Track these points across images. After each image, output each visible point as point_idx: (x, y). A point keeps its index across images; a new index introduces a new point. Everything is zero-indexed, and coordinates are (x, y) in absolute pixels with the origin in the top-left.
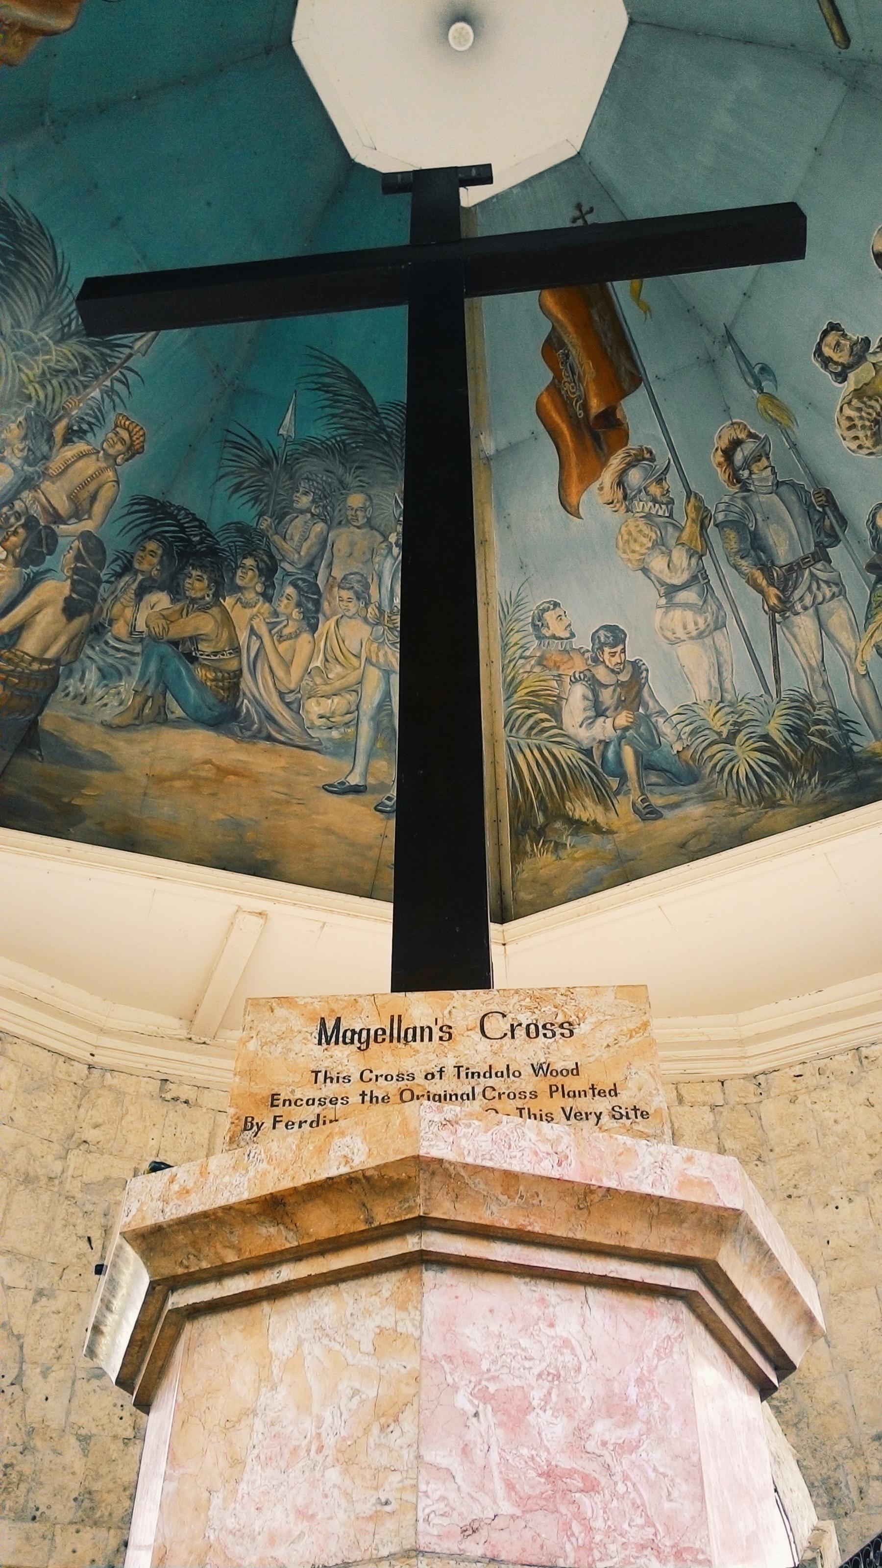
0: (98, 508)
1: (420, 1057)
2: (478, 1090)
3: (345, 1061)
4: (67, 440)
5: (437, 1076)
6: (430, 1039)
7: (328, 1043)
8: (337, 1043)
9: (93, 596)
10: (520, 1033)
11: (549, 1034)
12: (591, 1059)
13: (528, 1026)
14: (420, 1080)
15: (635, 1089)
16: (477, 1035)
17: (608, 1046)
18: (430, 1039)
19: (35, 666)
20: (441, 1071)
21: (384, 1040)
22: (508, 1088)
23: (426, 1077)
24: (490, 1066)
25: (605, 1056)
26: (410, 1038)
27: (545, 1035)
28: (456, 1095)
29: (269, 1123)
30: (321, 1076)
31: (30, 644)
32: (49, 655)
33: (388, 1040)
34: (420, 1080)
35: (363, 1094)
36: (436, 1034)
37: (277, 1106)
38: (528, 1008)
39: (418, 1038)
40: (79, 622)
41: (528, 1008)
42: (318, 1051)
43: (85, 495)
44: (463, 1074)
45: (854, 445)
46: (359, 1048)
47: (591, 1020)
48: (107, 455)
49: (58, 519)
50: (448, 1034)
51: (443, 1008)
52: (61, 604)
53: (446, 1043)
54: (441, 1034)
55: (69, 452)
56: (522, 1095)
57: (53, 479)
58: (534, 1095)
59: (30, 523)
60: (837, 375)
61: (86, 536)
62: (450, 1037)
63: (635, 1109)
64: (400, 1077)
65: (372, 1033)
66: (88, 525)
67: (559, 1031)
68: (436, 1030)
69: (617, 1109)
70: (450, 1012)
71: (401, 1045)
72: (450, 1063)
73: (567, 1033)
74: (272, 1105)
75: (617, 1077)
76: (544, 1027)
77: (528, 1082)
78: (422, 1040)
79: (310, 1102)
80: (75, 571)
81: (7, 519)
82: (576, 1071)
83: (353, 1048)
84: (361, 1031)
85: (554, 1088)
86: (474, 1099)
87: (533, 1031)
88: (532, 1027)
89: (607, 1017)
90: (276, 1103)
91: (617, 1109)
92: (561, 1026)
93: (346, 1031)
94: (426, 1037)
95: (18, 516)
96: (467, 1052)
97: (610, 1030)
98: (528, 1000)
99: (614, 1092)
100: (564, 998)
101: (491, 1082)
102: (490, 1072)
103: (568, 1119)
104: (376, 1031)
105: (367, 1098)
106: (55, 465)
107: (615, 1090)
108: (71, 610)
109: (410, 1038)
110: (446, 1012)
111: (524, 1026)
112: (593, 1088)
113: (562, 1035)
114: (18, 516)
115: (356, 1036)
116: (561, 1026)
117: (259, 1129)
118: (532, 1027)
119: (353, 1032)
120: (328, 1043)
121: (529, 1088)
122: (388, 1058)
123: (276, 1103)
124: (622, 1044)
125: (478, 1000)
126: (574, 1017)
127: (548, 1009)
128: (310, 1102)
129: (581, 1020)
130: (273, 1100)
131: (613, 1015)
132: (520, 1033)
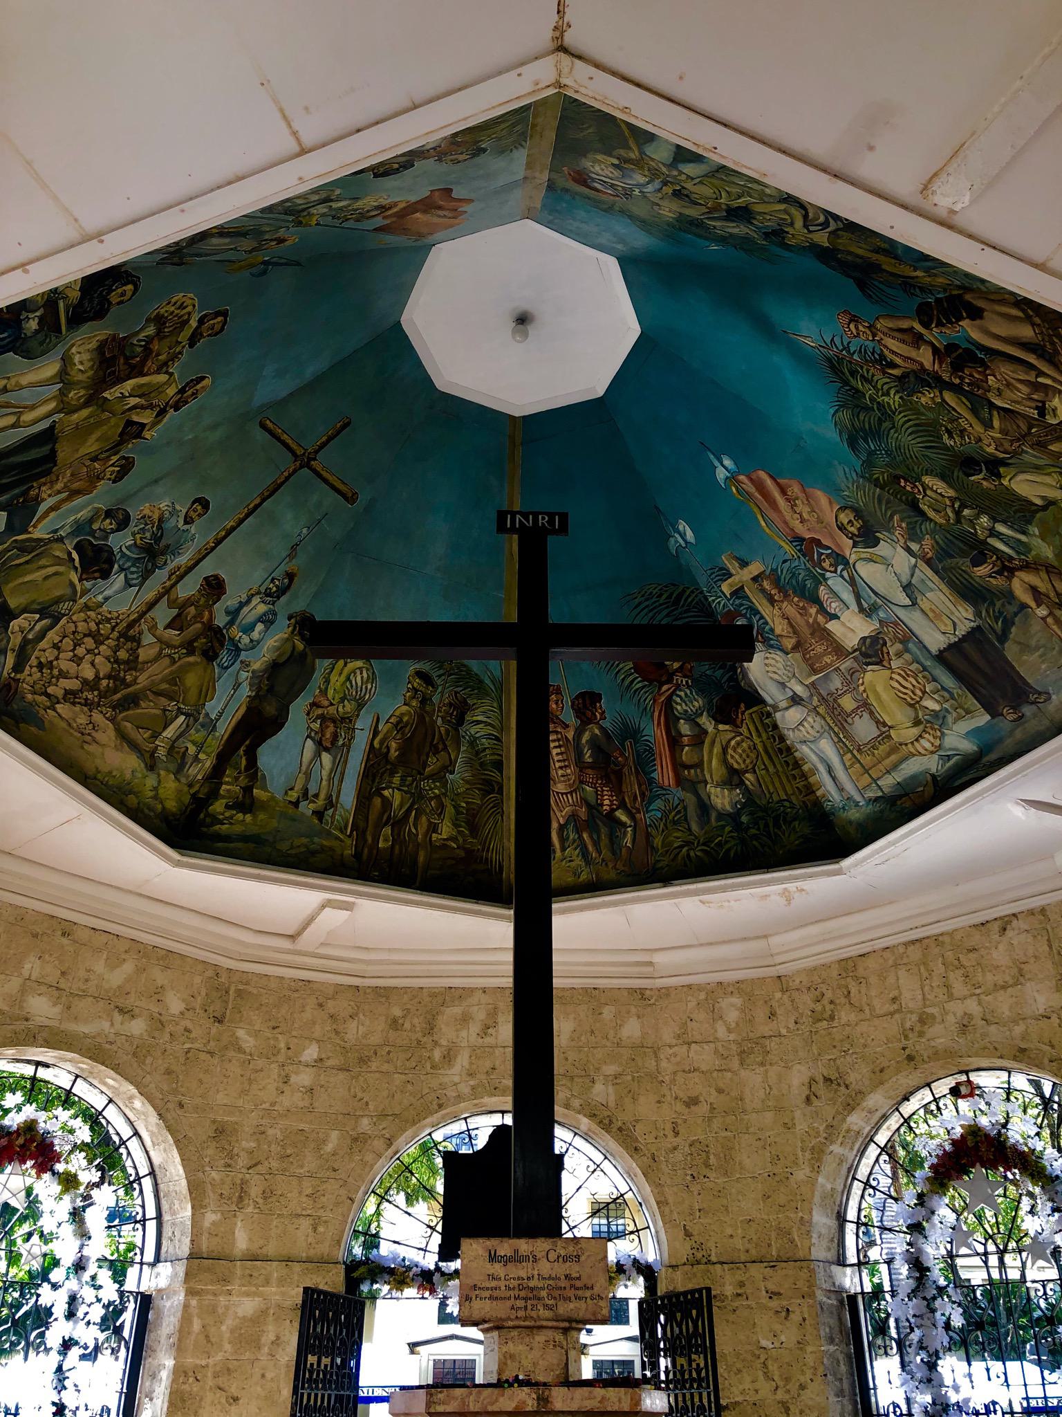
0: (905, 324)
4: (893, 365)
9: (951, 299)
19: (1037, 320)
31: (1027, 332)
32: (1021, 314)
40: (980, 303)
43: (905, 337)
45: (173, 300)
48: (874, 335)
49: (936, 351)
52: (978, 322)
55: (898, 361)
57: (921, 364)
59: (957, 368)
60: (205, 316)
61: (926, 325)
66: (918, 327)
80: (951, 323)
81: (969, 385)
95: (962, 378)
106: (916, 367)
108: (976, 314)
114: (962, 378)
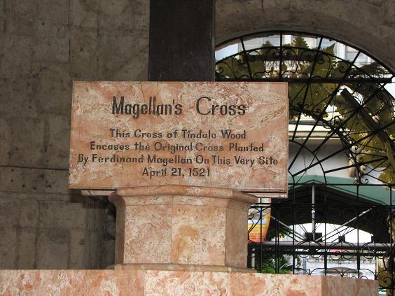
1: (165, 124)
2: (194, 144)
3: (127, 124)
5: (174, 135)
6: (170, 113)
7: (118, 113)
8: (122, 113)
10: (217, 111)
11: (232, 113)
12: (252, 129)
13: (222, 107)
14: (164, 138)
15: (272, 147)
16: (194, 112)
17: (262, 121)
18: (170, 113)
20: (175, 133)
21: (146, 112)
22: (209, 144)
23: (168, 136)
24: (201, 131)
25: (260, 127)
26: (160, 112)
27: (230, 113)
28: (183, 147)
29: (90, 159)
30: (115, 132)
33: (148, 112)
34: (164, 138)
35: (136, 144)
36: (174, 110)
37: (94, 149)
38: (222, 95)
39: (164, 112)
41: (222, 95)
42: (112, 118)
44: (186, 135)
46: (134, 117)
47: (255, 104)
50: (179, 110)
51: (178, 94)
53: (178, 116)
54: (176, 110)
56: (215, 148)
58: (222, 148)
62: (181, 113)
63: (271, 159)
64: (155, 135)
65: (140, 107)
67: (238, 111)
68: (173, 107)
69: (262, 158)
70: (181, 96)
71: (155, 116)
72: (180, 127)
73: (241, 111)
74: (92, 148)
75: (264, 140)
76: (230, 108)
77: (219, 142)
78: (166, 113)
79: (110, 147)
82: (243, 136)
83: (130, 117)
84: (135, 105)
85: (232, 145)
86: (191, 150)
87: (225, 110)
88: (224, 107)
89: (265, 103)
90: (93, 147)
91: (262, 158)
92: (239, 108)
93: (126, 106)
94: (168, 112)
96: (189, 122)
97: (264, 111)
98: (223, 90)
99: (262, 148)
100: (242, 90)
101: (201, 140)
102: (200, 134)
103: (237, 163)
104: (142, 106)
105: (138, 147)
107: (262, 148)
109: (160, 112)
110: (179, 96)
111: (219, 107)
112: (252, 146)
113: (239, 113)
115: (132, 109)
116: (239, 108)
117: (86, 160)
118: (224, 107)
119: (130, 106)
120: (118, 113)
121: (220, 145)
122: (148, 123)
123: (93, 147)
124: (270, 120)
125: (196, 89)
126: (246, 102)
127: (233, 97)
128: (110, 147)
129: (250, 104)
130: (92, 145)
131: (267, 102)
132: (217, 111)
